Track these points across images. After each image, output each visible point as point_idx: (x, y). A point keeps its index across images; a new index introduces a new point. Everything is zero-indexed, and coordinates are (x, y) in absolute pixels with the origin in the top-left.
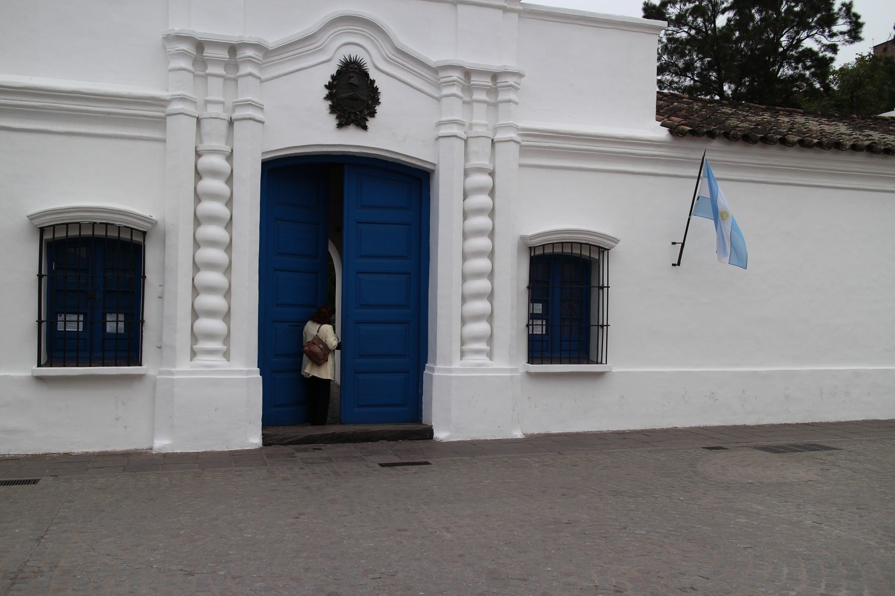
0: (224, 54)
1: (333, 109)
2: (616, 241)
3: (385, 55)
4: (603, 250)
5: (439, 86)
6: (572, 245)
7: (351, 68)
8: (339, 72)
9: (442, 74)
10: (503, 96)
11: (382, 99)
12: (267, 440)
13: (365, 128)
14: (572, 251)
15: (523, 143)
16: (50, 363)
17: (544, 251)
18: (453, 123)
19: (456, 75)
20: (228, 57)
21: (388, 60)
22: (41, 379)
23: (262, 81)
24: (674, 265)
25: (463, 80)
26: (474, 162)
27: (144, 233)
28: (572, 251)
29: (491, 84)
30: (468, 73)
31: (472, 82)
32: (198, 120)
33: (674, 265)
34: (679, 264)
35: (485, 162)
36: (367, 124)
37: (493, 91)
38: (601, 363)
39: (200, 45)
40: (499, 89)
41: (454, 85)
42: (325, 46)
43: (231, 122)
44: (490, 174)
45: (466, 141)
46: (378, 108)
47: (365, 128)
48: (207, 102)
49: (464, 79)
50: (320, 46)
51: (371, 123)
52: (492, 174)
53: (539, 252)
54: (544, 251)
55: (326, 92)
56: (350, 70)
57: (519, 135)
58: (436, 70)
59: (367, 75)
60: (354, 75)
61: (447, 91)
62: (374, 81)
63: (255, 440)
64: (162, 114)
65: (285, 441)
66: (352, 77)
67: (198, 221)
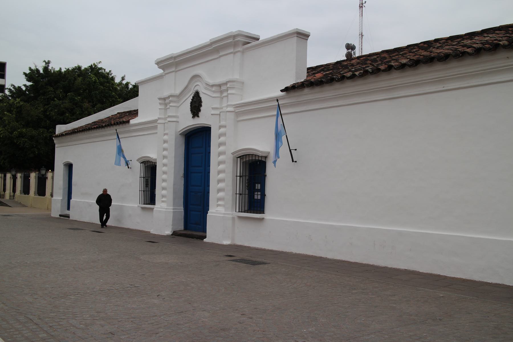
10: (229, 92)
11: (203, 104)
12: (175, 234)
15: (236, 111)
21: (206, 89)
22: (143, 208)
23: (178, 107)
51: (200, 114)
57: (234, 108)
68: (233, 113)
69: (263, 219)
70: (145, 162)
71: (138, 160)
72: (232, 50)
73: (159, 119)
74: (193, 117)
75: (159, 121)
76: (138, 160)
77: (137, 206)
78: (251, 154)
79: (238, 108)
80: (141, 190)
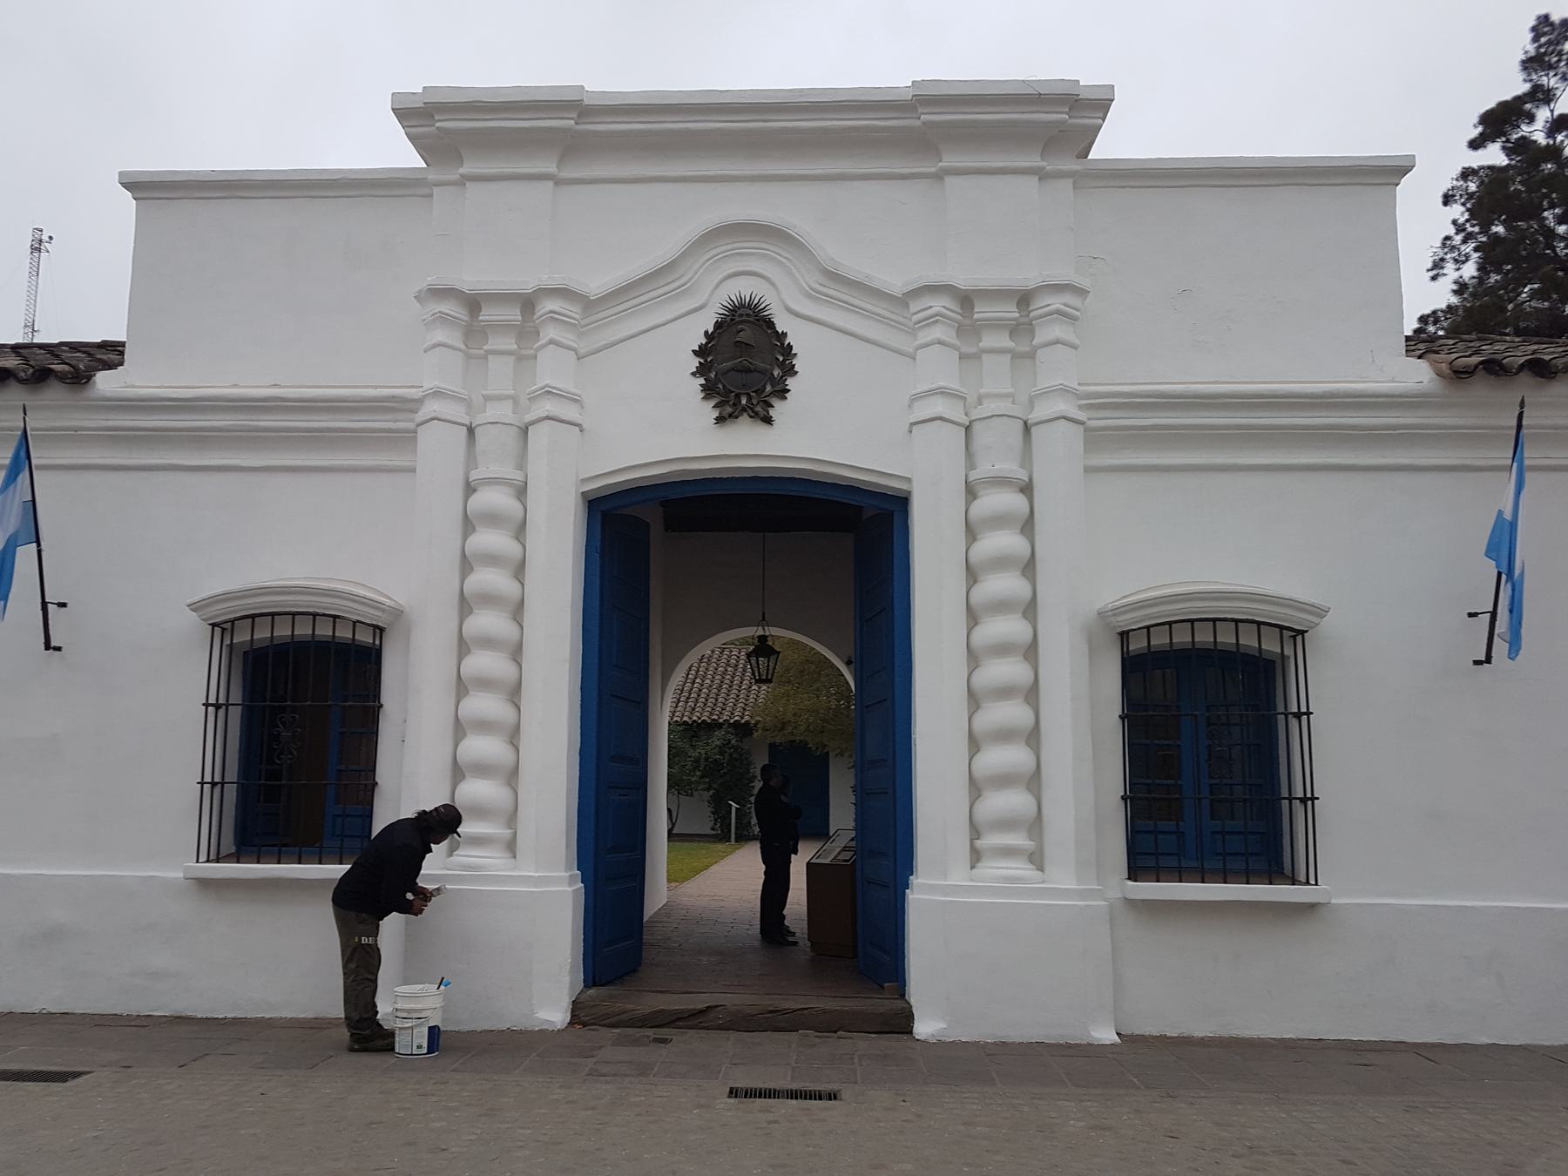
0: (514, 314)
1: (709, 391)
2: (1321, 612)
3: (808, 289)
4: (1294, 634)
5: (912, 332)
6: (1214, 625)
7: (741, 315)
8: (718, 325)
9: (914, 307)
11: (798, 364)
13: (768, 420)
14: (334, 632)
16: (237, 857)
17: (293, 631)
18: (934, 394)
19: (939, 304)
20: (520, 318)
21: (814, 296)
22: (206, 885)
24: (1477, 663)
25: (958, 313)
26: (984, 469)
27: (379, 630)
28: (334, 632)
29: (1017, 315)
30: (966, 299)
31: (976, 316)
32: (471, 431)
33: (1477, 663)
34: (1488, 660)
35: (1010, 467)
36: (772, 412)
37: (1021, 329)
38: (1308, 883)
39: (474, 303)
40: (1034, 322)
41: (937, 321)
42: (693, 284)
43: (524, 431)
44: (1022, 491)
45: (968, 429)
46: (791, 383)
47: (768, 420)
48: (487, 398)
49: (960, 311)
50: (685, 284)
51: (779, 410)
52: (1027, 489)
53: (1138, 644)
54: (293, 631)
55: (695, 362)
56: (738, 319)
57: (1080, 407)
58: (903, 301)
59: (771, 325)
60: (747, 328)
61: (926, 336)
62: (784, 335)
63: (554, 1014)
64: (411, 425)
65: (613, 1020)
66: (742, 330)
67: (465, 606)
68: (1081, 428)
69: (1309, 909)
70: (228, 626)
71: (194, 607)
72: (1034, 161)
73: (437, 394)
74: (720, 420)
75: (431, 408)
76: (194, 607)
77: (181, 875)
78: (1253, 622)
79: (1107, 413)
80: (208, 778)
